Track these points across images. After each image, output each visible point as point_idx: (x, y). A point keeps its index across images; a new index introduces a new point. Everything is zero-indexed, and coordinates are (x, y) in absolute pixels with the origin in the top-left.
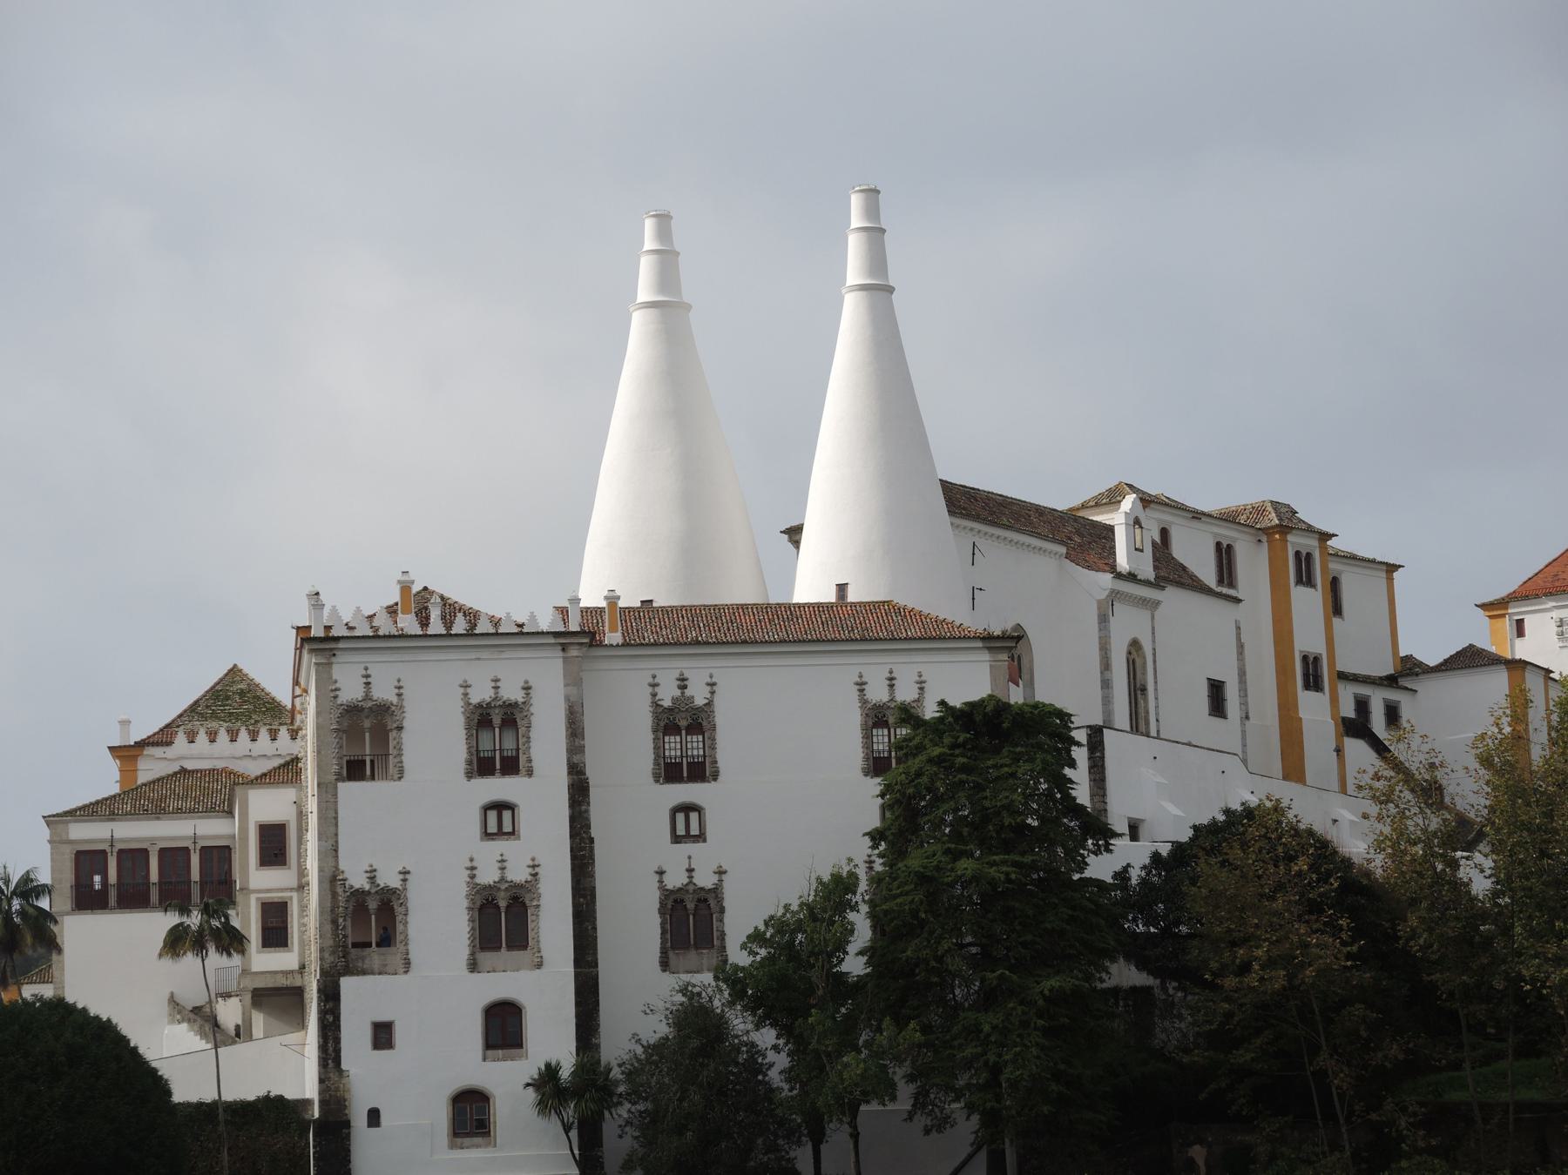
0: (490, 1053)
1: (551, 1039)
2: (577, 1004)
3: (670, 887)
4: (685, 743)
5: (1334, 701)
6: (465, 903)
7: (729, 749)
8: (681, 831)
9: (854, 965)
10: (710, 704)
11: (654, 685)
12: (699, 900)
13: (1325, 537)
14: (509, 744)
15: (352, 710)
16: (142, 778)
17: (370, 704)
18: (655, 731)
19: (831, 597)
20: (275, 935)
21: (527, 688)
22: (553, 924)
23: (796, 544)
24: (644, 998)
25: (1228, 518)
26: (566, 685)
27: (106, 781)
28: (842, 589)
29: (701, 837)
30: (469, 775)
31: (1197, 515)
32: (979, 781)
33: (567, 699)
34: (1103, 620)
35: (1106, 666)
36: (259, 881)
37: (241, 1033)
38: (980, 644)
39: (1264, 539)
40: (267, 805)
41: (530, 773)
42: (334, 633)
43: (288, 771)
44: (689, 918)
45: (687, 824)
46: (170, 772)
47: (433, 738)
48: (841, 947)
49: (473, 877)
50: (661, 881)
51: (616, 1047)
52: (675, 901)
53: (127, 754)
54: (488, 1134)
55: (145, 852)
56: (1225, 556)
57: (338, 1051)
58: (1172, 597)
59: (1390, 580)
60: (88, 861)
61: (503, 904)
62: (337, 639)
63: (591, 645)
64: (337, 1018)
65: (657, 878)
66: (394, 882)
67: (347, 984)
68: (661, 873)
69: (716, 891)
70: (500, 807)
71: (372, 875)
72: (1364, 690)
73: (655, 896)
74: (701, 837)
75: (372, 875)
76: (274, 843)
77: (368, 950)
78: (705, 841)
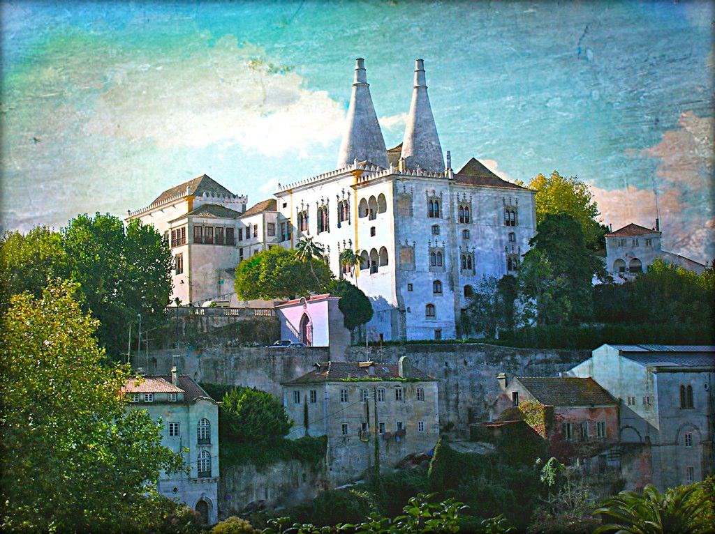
21: (441, 194)
41: (442, 218)
60: (196, 228)
61: (436, 253)
70: (435, 226)
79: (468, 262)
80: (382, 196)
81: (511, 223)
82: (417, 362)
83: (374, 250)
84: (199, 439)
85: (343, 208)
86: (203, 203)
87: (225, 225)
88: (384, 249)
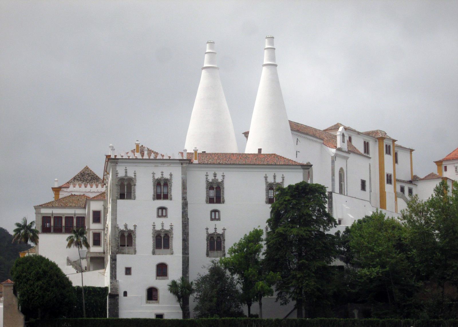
0: (158, 277)
1: (175, 274)
2: (183, 265)
3: (210, 233)
4: (216, 193)
5: (395, 187)
6: (152, 235)
7: (228, 194)
8: (213, 217)
9: (262, 257)
10: (223, 181)
11: (207, 175)
12: (218, 237)
13: (394, 141)
14: (165, 191)
15: (122, 180)
16: (61, 197)
17: (127, 178)
18: (207, 189)
19: (256, 152)
20: (97, 242)
21: (171, 175)
22: (177, 242)
23: (247, 137)
24: (202, 265)
25: (368, 134)
26: (182, 174)
27: (50, 197)
28: (260, 150)
29: (219, 219)
30: (154, 199)
31: (359, 133)
32: (298, 205)
33: (182, 178)
34: (333, 162)
35: (333, 175)
36: (93, 227)
37: (87, 269)
38: (300, 167)
39: (377, 140)
40: (96, 206)
41: (171, 199)
42: (117, 158)
43: (102, 197)
44: (215, 242)
45: (215, 215)
46: (68, 195)
47: (144, 188)
48: (258, 250)
49: (154, 228)
50: (207, 231)
51: (193, 277)
52: (211, 237)
53: (57, 190)
54: (157, 300)
55: (61, 218)
56: (366, 145)
57: (116, 275)
58: (352, 157)
59: (411, 154)
61: (162, 236)
62: (118, 159)
63: (189, 163)
64: (116, 266)
65: (206, 230)
66: (132, 228)
67: (119, 257)
68: (207, 229)
69: (223, 235)
70: (162, 208)
71: (126, 226)
72: (403, 184)
73: (205, 236)
74: (219, 219)
75: (126, 226)
76: (97, 217)
77: (124, 247)
78: (220, 220)
86: (70, 194)
87: (75, 214)
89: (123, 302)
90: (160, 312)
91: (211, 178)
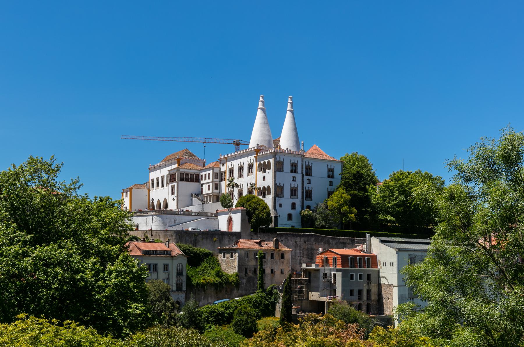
29: (310, 183)
41: (297, 173)
67: (277, 198)
69: (312, 191)
70: (294, 177)
74: (310, 183)
79: (308, 195)
80: (269, 162)
81: (331, 176)
82: (282, 241)
83: (264, 187)
84: (177, 273)
85: (250, 166)
88: (269, 187)
89: (280, 220)
90: (293, 224)
91: (307, 164)
